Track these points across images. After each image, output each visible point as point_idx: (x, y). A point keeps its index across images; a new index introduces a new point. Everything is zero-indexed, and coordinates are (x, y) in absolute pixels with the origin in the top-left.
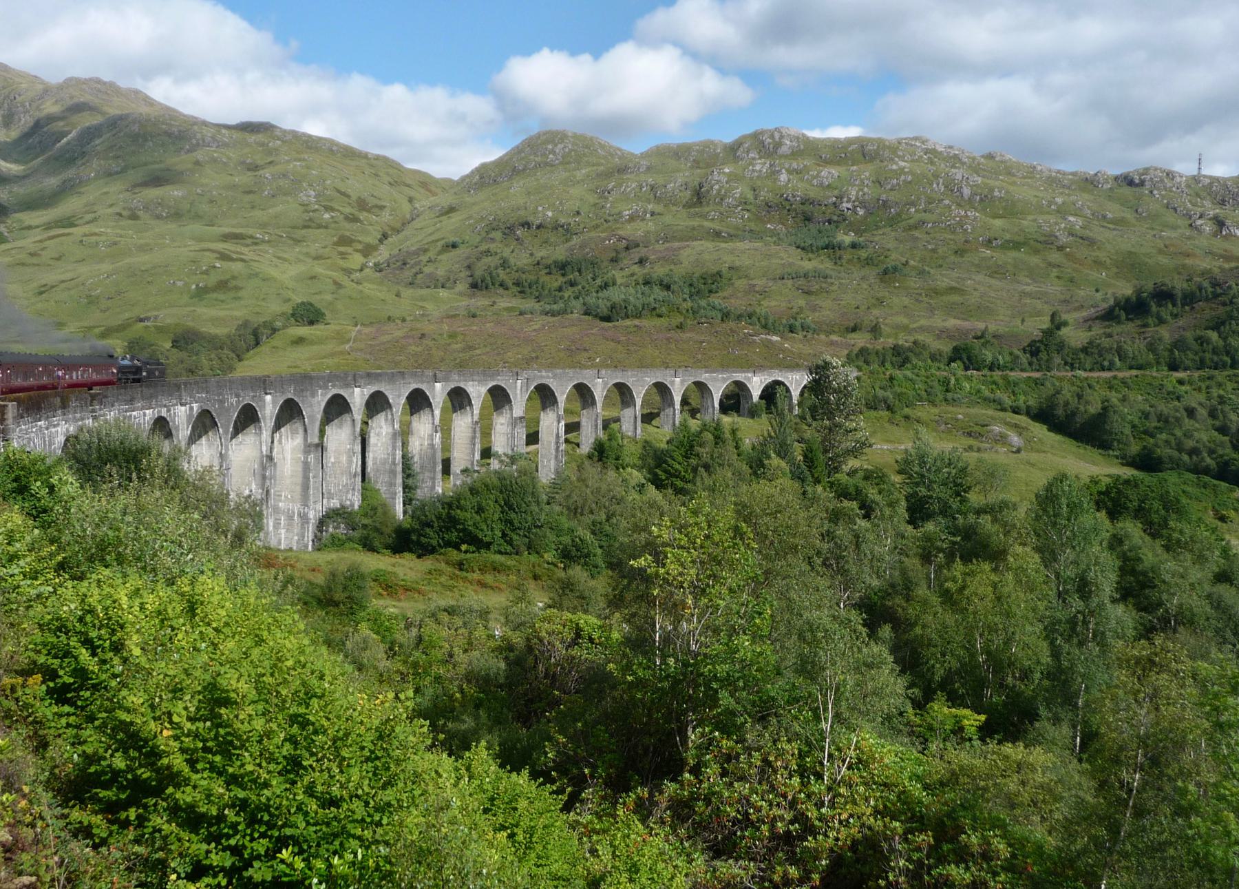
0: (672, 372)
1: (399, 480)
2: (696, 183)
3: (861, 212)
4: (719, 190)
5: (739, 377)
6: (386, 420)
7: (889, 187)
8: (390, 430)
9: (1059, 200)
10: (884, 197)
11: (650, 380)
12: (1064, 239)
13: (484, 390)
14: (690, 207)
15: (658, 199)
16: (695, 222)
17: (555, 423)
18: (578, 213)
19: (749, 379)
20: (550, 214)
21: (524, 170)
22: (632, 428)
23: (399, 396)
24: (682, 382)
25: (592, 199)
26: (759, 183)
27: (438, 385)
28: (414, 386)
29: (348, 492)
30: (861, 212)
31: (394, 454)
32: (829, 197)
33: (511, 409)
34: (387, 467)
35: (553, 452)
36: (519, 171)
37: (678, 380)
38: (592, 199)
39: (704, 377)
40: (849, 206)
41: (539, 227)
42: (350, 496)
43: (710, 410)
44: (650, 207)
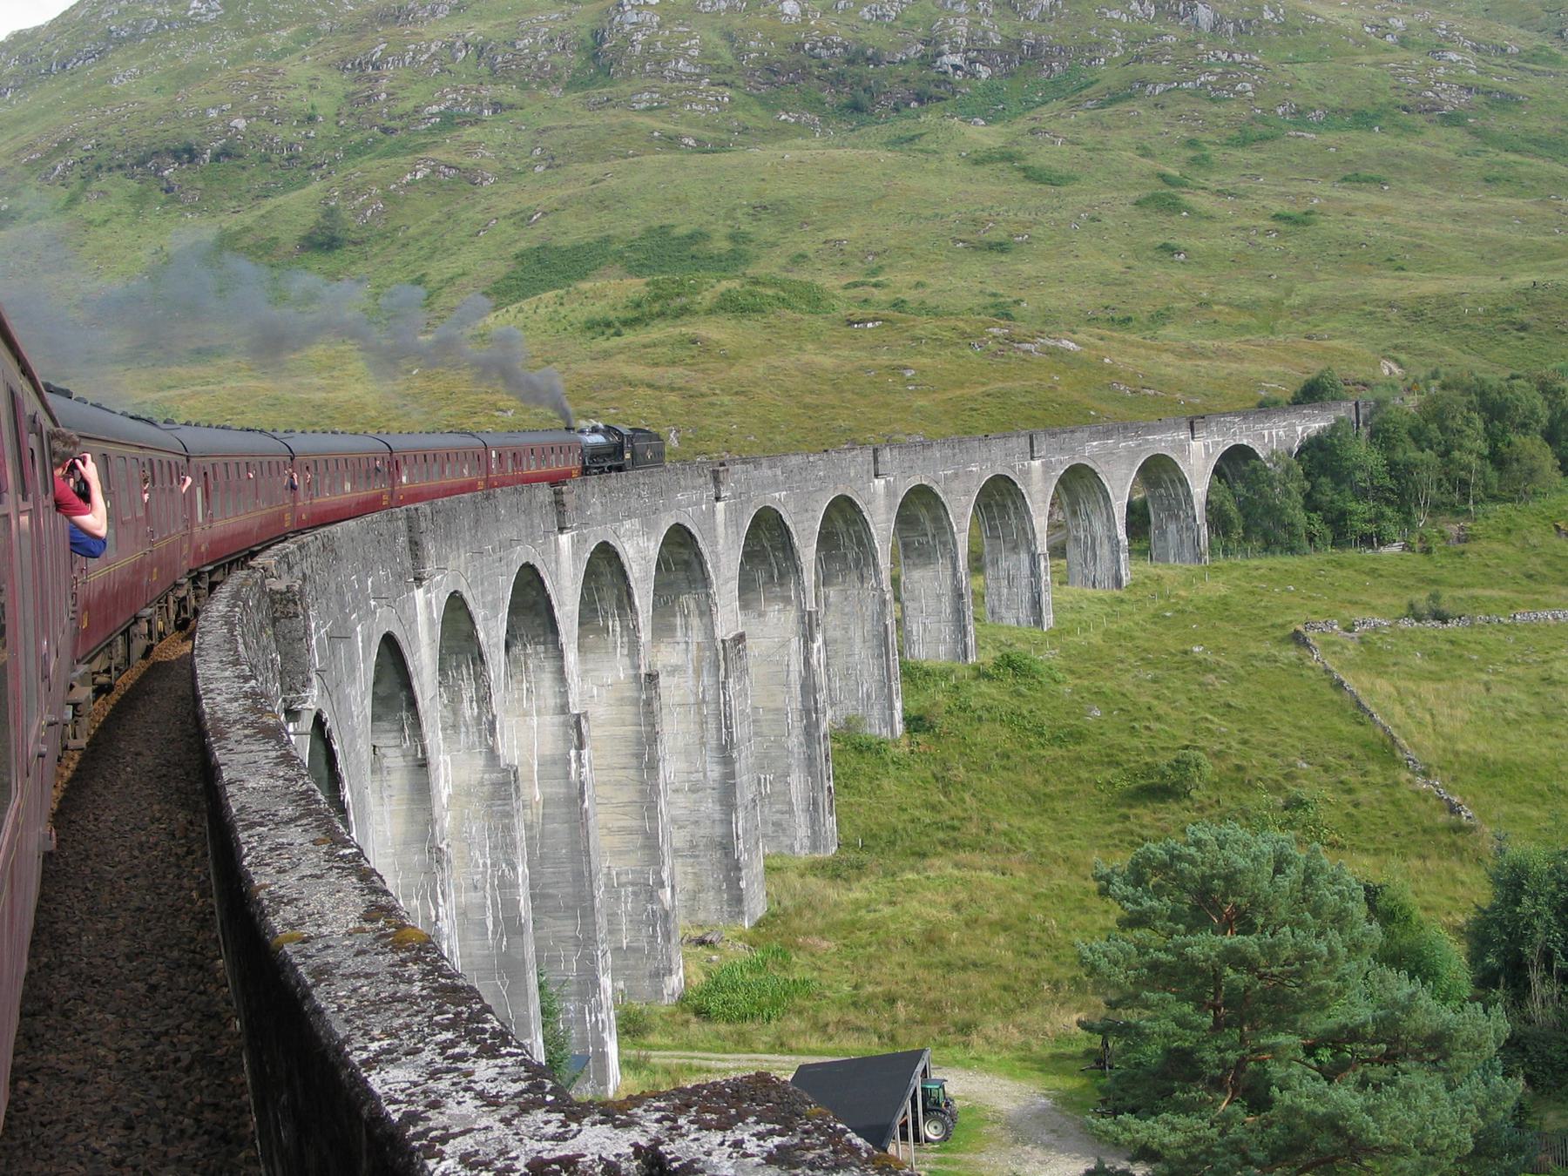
0: (1024, 442)
2: (585, 33)
3: (984, 72)
4: (649, 44)
5: (1161, 442)
7: (1034, 13)
9: (1398, 23)
10: (1029, 37)
11: (981, 472)
12: (1453, 100)
13: (653, 548)
14: (584, 86)
15: (498, 74)
16: (613, 117)
17: (795, 644)
18: (311, 119)
19: (1182, 447)
20: (240, 123)
21: (133, 38)
22: (947, 631)
23: (495, 607)
24: (1047, 467)
25: (338, 84)
26: (738, 22)
27: (565, 539)
30: (984, 72)
31: (506, 886)
32: (905, 44)
33: (707, 612)
35: (795, 741)
36: (121, 41)
37: (1037, 463)
38: (338, 84)
39: (1089, 451)
40: (957, 59)
41: (224, 154)
43: (1104, 551)
44: (488, 92)
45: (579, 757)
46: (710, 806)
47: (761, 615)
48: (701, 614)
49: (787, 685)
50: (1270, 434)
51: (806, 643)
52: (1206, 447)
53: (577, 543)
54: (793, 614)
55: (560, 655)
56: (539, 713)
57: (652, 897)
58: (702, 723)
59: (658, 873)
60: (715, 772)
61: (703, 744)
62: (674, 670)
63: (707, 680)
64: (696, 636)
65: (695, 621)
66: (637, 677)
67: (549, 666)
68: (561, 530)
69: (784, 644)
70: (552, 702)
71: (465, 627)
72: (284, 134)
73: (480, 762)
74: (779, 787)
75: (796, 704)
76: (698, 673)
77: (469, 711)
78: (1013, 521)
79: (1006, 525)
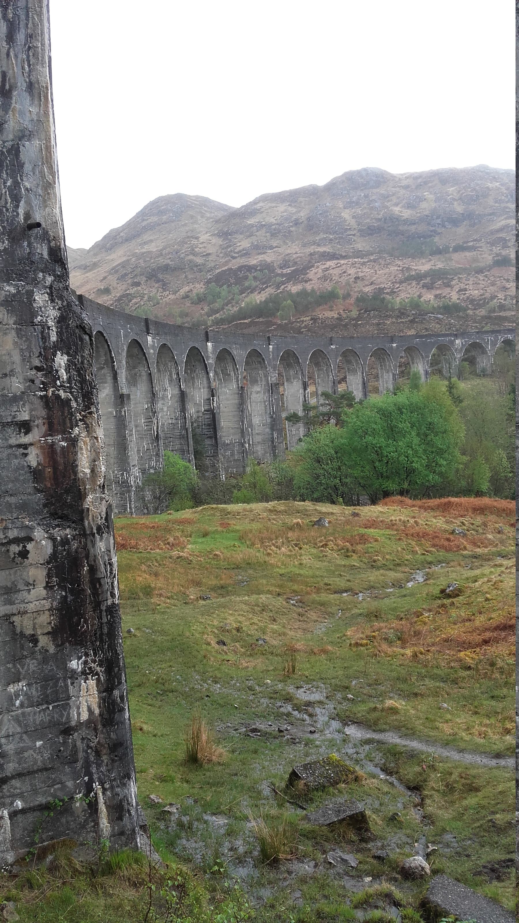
1: (191, 449)
6: (171, 380)
8: (176, 391)
17: (301, 391)
19: (452, 342)
27: (209, 344)
28: (191, 344)
29: (150, 459)
33: (266, 376)
34: (177, 432)
40: (439, 221)
42: (153, 463)
45: (213, 400)
46: (268, 430)
47: (292, 383)
48: (265, 377)
49: (299, 402)
50: (488, 339)
51: (304, 391)
52: (462, 343)
53: (214, 347)
54: (301, 382)
55: (208, 373)
56: (203, 388)
57: (243, 446)
58: (266, 406)
59: (244, 440)
60: (269, 420)
61: (266, 413)
62: (258, 392)
63: (267, 395)
64: (264, 383)
65: (263, 379)
66: (239, 387)
67: (205, 376)
68: (207, 341)
69: (298, 391)
70: (206, 385)
71: (171, 355)
72: (199, 260)
73: (177, 389)
74: (297, 432)
75: (302, 408)
76: (264, 393)
77: (175, 377)
78: (387, 363)
79: (385, 365)
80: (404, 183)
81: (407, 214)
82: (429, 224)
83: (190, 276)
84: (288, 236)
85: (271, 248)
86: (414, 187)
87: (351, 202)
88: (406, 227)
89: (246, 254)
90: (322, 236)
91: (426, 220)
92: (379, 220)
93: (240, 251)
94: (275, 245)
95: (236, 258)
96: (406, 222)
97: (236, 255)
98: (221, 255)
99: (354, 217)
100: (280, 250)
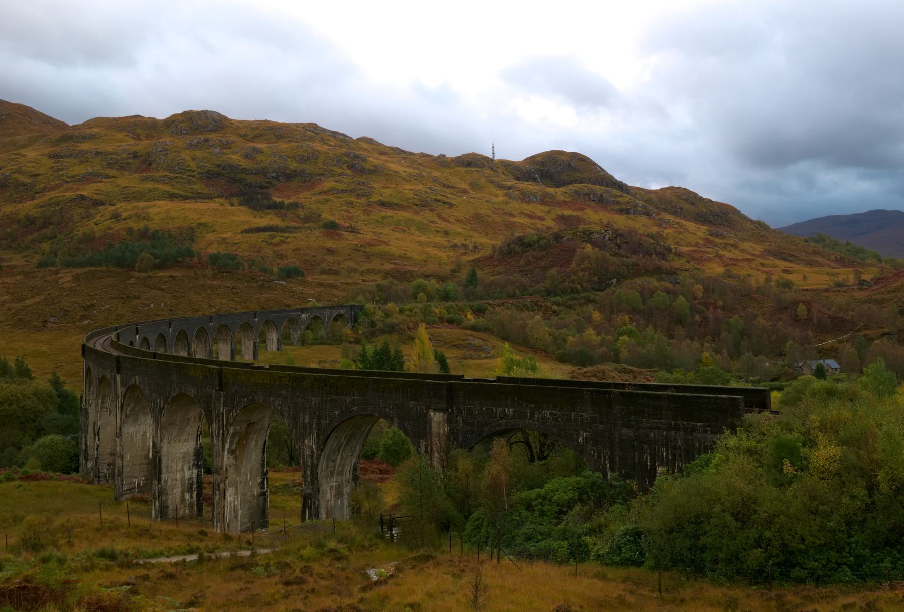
19: (299, 316)
40: (274, 175)
80: (243, 132)
81: (244, 164)
82: (264, 176)
83: (14, 196)
84: (123, 167)
85: (107, 177)
86: (250, 136)
87: (192, 145)
88: (243, 176)
89: (80, 180)
90: (162, 173)
91: (263, 172)
92: (219, 166)
93: (73, 177)
94: (111, 174)
95: (68, 182)
96: (244, 171)
97: (69, 180)
98: (52, 178)
99: (194, 159)
100: (119, 181)
